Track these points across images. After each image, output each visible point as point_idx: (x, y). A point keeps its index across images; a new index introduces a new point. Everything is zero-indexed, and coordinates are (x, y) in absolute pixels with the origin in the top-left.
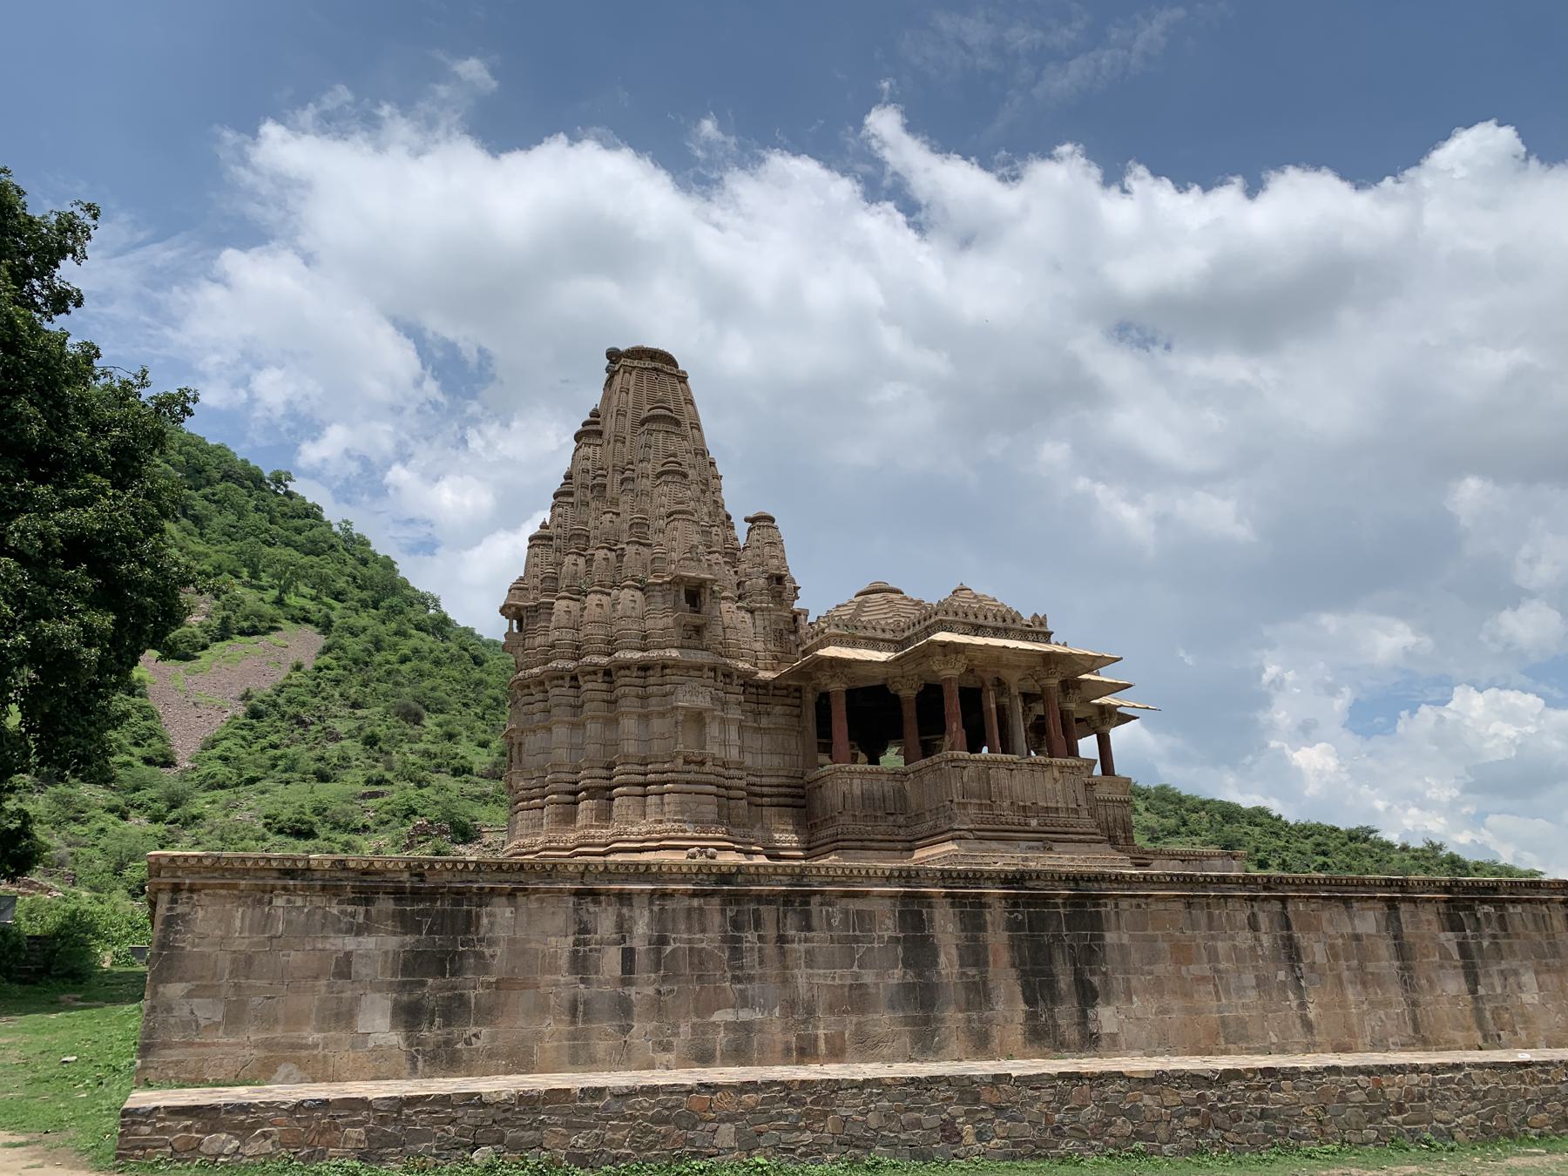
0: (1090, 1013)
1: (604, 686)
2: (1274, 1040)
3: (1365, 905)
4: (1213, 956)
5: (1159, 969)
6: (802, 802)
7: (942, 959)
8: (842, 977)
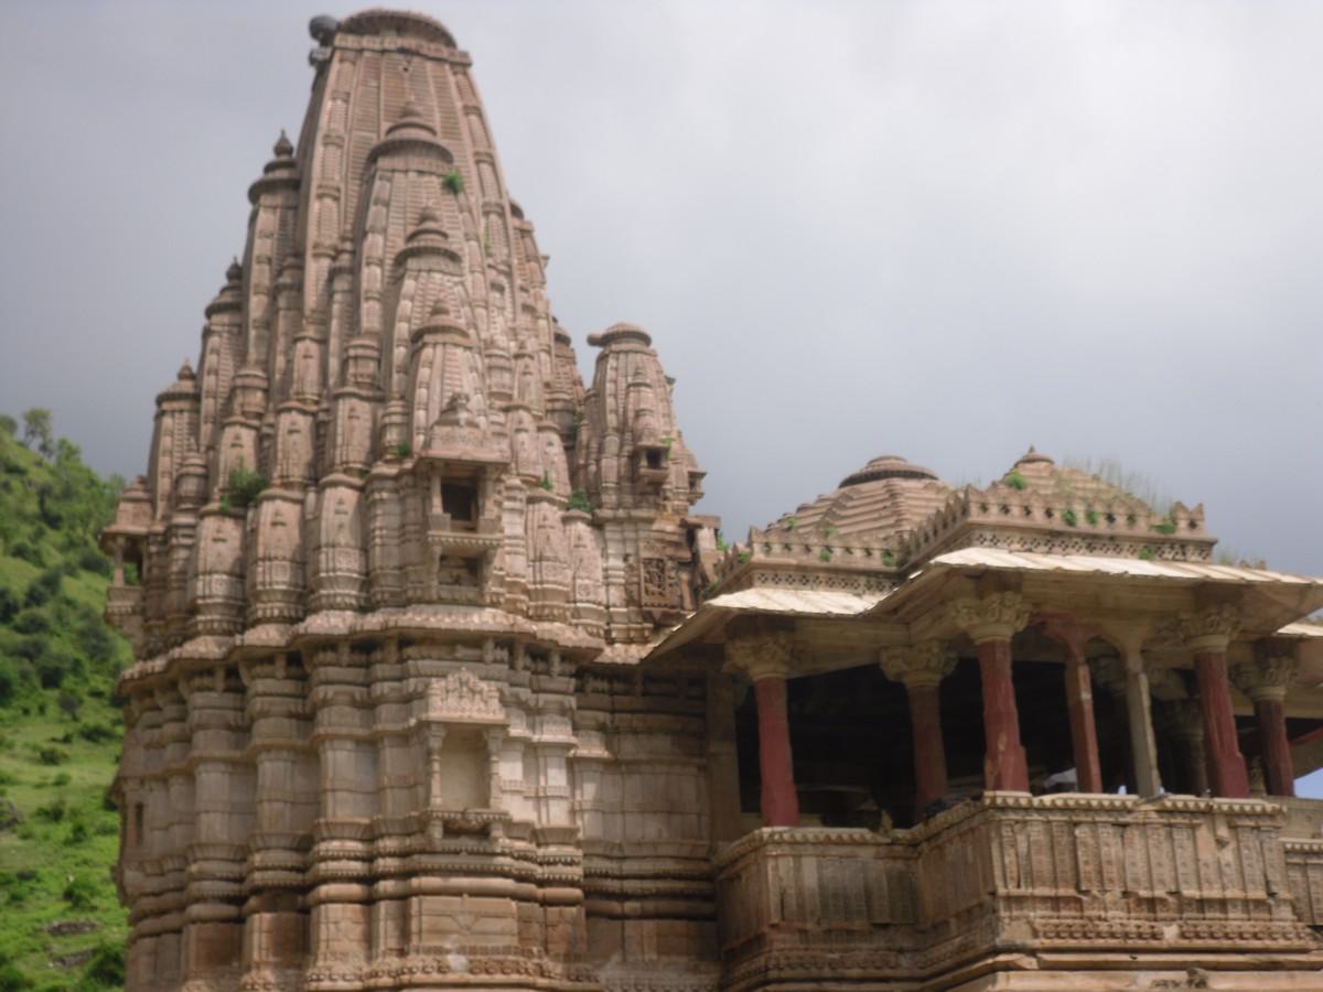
1: (289, 686)
6: (707, 908)
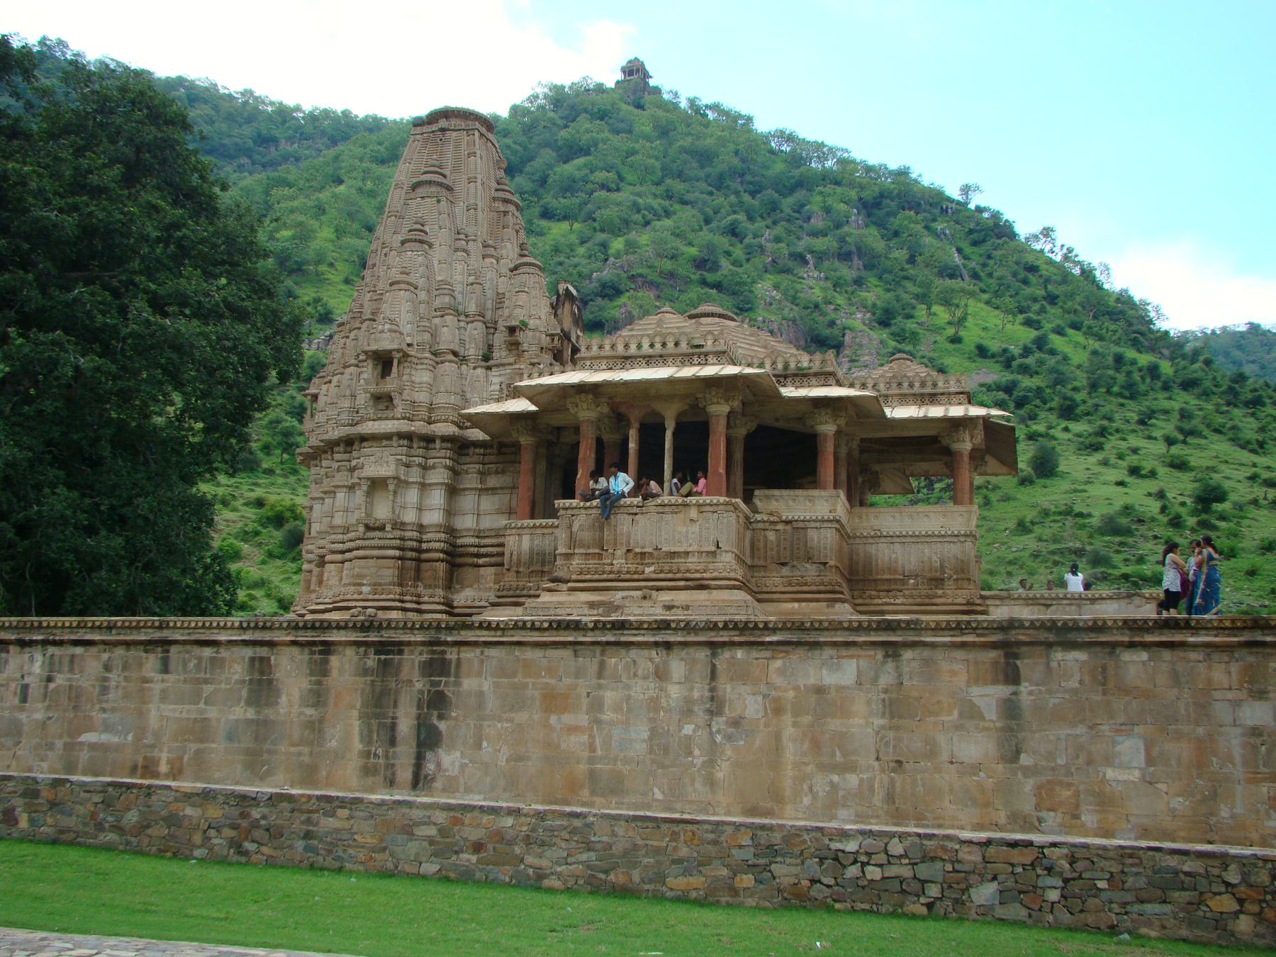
0: (429, 755)
2: (659, 796)
3: (844, 652)
4: (596, 706)
5: (521, 717)
6: (498, 559)
7: (283, 699)
8: (188, 711)
